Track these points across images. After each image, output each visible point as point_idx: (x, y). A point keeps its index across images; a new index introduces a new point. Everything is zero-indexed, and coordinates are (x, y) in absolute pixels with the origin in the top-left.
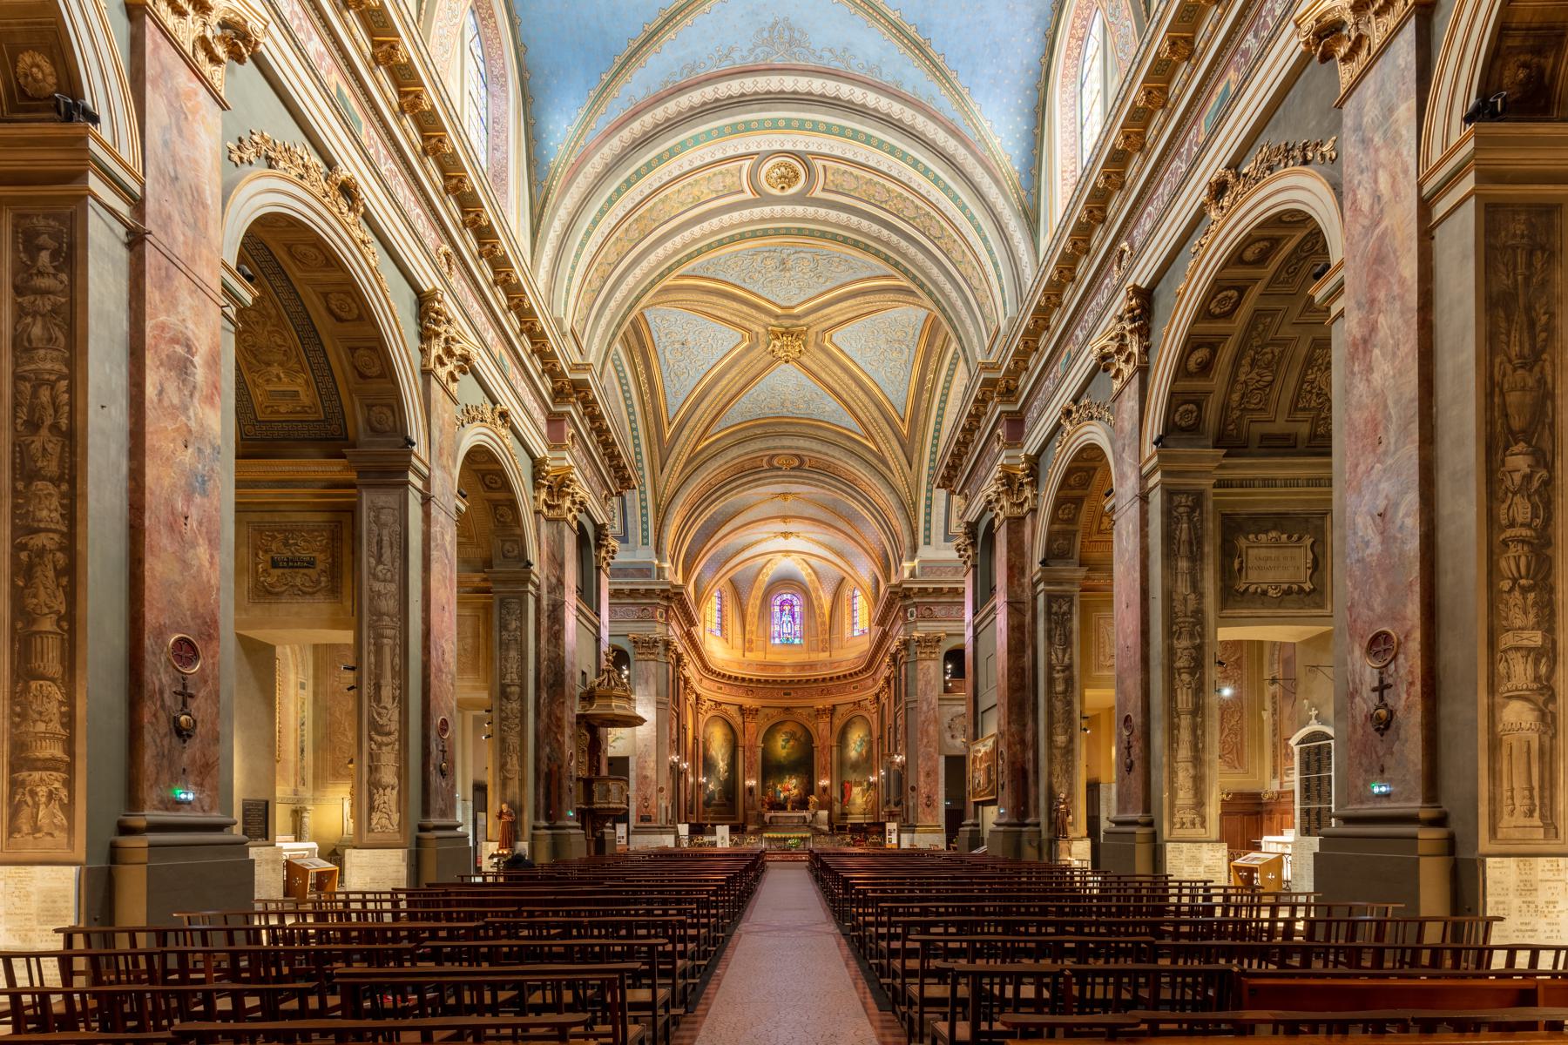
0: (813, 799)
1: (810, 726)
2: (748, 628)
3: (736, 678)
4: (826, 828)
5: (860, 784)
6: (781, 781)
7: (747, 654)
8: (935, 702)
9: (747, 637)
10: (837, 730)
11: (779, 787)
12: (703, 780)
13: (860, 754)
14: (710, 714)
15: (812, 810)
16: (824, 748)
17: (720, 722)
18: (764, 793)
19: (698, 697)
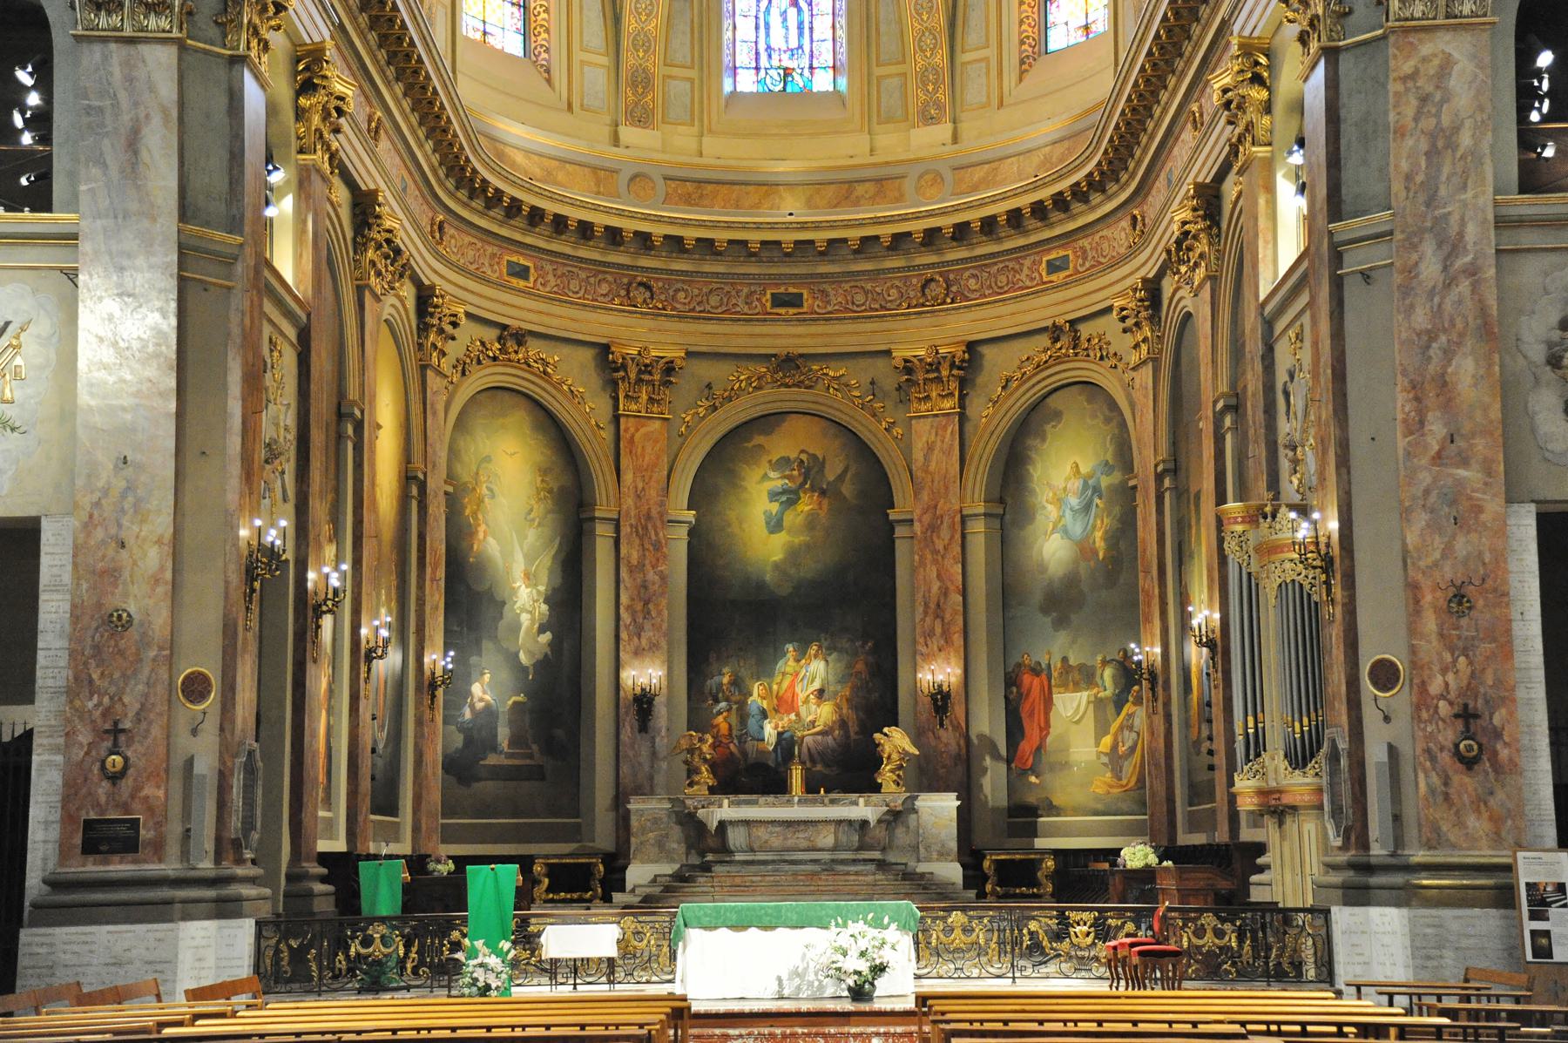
0: (896, 741)
3: (585, 230)
4: (952, 872)
5: (1087, 677)
6: (765, 669)
7: (628, 133)
10: (985, 450)
11: (757, 697)
12: (437, 659)
13: (1084, 549)
14: (481, 378)
15: (892, 790)
17: (519, 418)
18: (698, 721)
19: (425, 298)
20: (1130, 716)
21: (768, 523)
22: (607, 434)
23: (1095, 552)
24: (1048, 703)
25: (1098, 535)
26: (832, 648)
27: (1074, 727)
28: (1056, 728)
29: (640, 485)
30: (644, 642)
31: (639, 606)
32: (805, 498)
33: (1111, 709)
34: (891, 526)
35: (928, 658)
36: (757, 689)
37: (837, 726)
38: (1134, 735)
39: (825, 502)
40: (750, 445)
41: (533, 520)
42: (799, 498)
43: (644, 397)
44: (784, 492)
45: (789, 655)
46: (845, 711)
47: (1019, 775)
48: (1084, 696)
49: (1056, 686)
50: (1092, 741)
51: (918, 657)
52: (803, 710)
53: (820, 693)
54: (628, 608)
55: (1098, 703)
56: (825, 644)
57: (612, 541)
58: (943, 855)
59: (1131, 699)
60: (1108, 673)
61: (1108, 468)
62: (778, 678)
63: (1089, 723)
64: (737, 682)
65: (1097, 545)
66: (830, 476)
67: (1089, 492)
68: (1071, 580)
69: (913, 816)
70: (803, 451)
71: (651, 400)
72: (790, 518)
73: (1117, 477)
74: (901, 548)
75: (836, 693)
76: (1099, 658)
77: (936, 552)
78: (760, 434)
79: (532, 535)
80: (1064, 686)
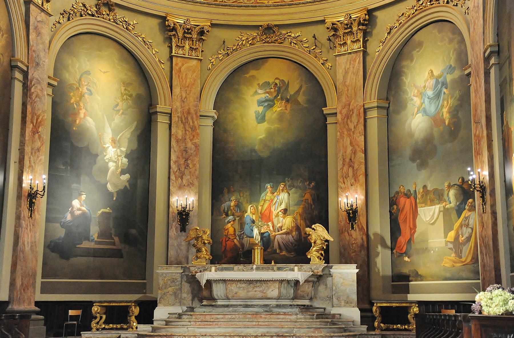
11: (250, 213)
13: (436, 120)
16: (348, 116)
20: (467, 218)
21: (257, 118)
22: (166, 67)
23: (443, 121)
24: (415, 213)
25: (445, 110)
26: (292, 186)
27: (431, 226)
28: (420, 228)
29: (184, 95)
30: (184, 181)
31: (182, 161)
32: (277, 104)
33: (454, 215)
34: (325, 117)
35: (344, 190)
36: (249, 209)
37: (294, 230)
38: (469, 230)
39: (289, 106)
40: (247, 76)
41: (119, 111)
42: (275, 104)
43: (187, 47)
44: (267, 101)
45: (268, 190)
46: (299, 221)
47: (399, 256)
48: (436, 208)
49: (420, 203)
50: (443, 235)
51: (339, 190)
52: (275, 221)
53: (285, 211)
54: (175, 162)
55: (446, 212)
56: (288, 184)
57: (167, 126)
58: (348, 303)
59: (467, 207)
60: (452, 193)
61: (451, 69)
62: (262, 203)
63: (440, 224)
64: (238, 205)
65: (444, 116)
66: (292, 91)
67: (440, 86)
68: (428, 140)
69: (330, 279)
70: (277, 79)
71: (191, 49)
72: (269, 115)
73: (457, 74)
74: (330, 129)
75: (294, 211)
76: (446, 184)
77: (349, 130)
78: (253, 69)
79: (118, 119)
80: (425, 203)
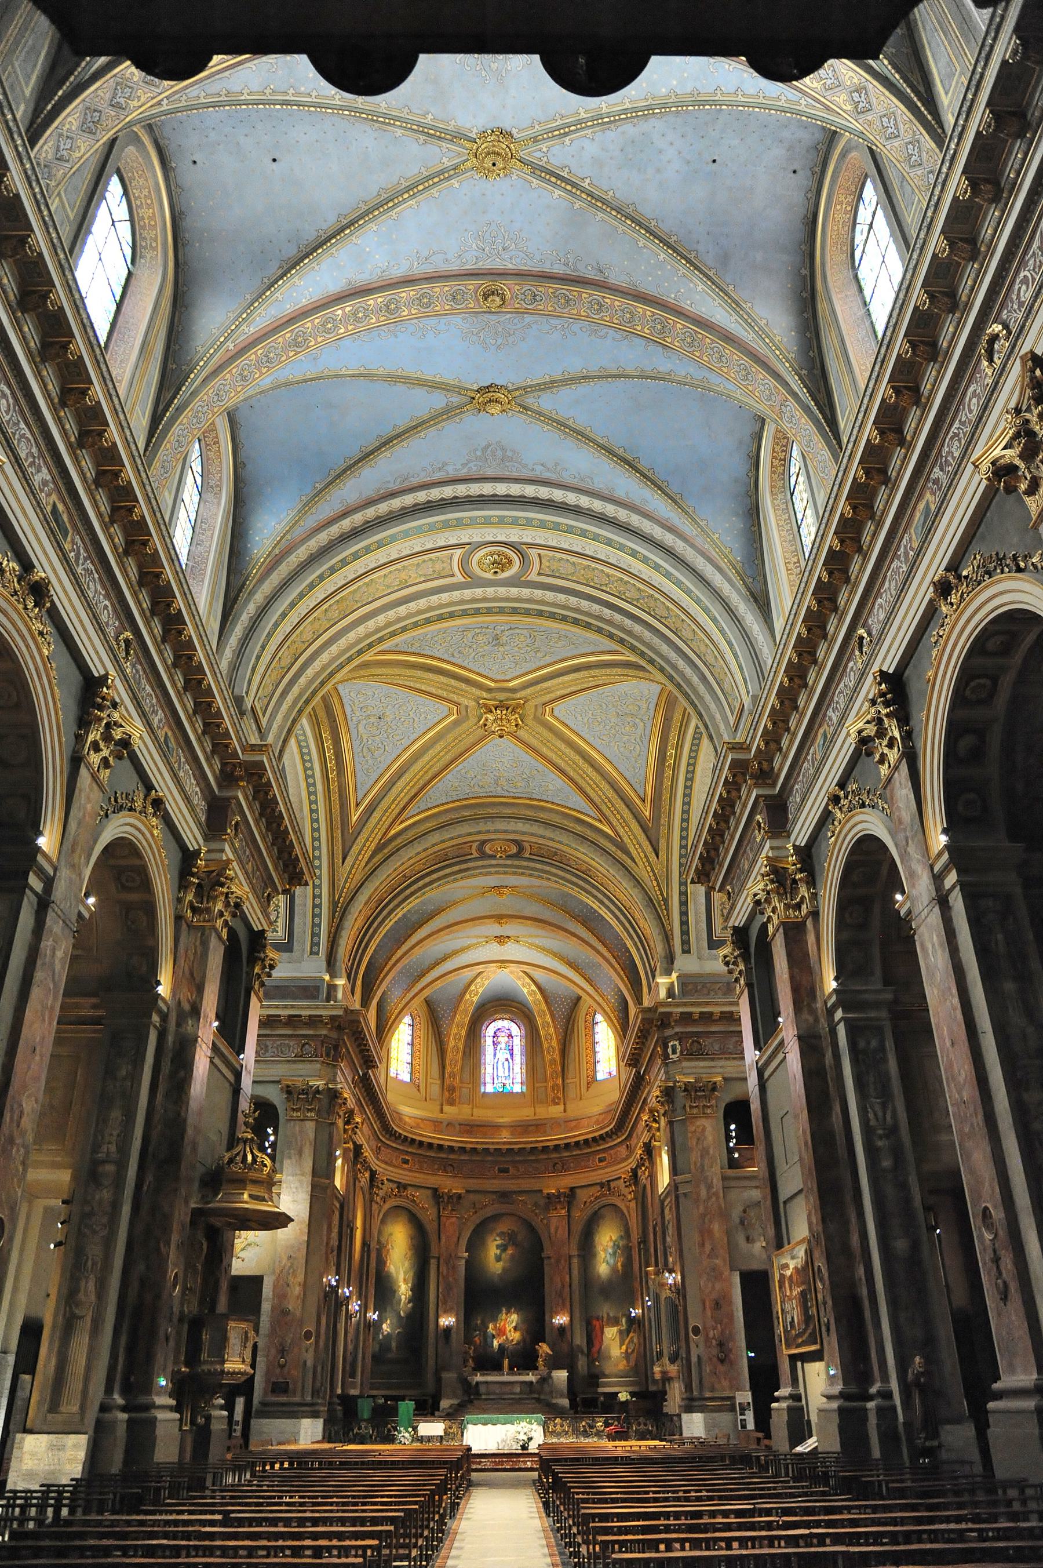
0: (544, 1348)
1: (536, 1222)
2: (448, 1069)
4: (565, 1402)
5: (615, 1322)
6: (494, 1319)
8: (717, 1183)
9: (447, 1082)
10: (578, 1228)
13: (614, 1269)
15: (542, 1369)
18: (468, 1340)
19: (373, 1174)
